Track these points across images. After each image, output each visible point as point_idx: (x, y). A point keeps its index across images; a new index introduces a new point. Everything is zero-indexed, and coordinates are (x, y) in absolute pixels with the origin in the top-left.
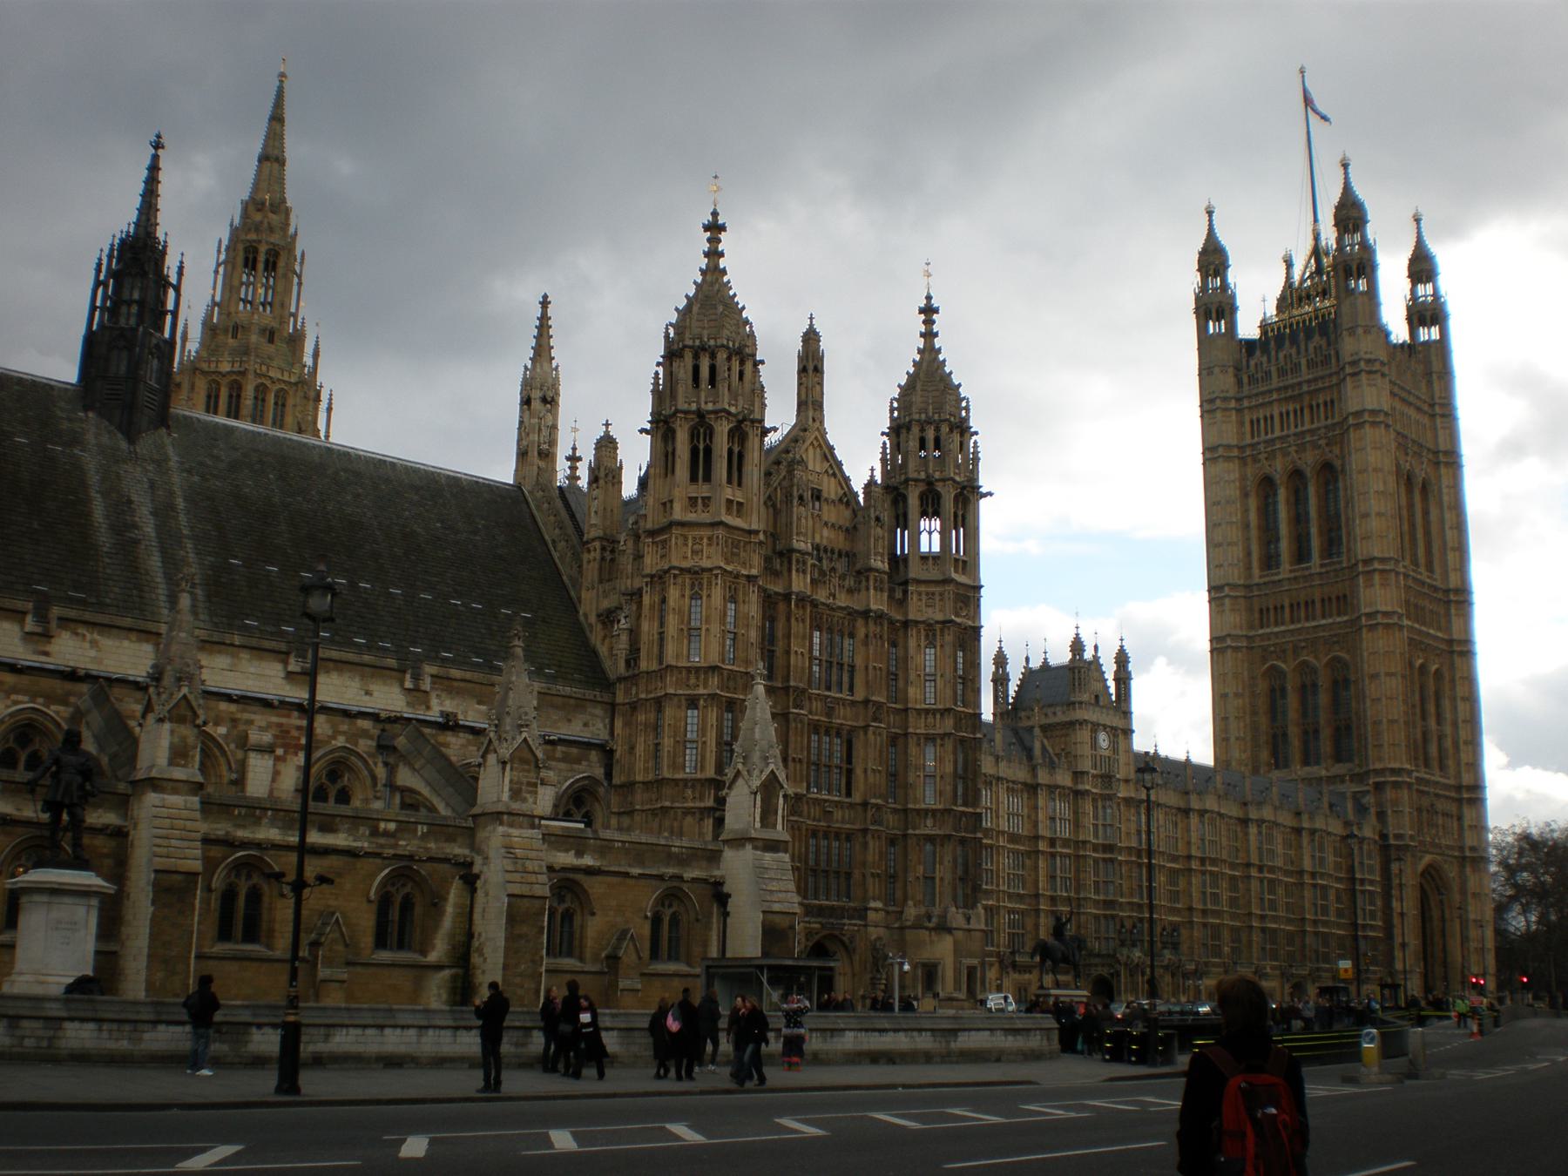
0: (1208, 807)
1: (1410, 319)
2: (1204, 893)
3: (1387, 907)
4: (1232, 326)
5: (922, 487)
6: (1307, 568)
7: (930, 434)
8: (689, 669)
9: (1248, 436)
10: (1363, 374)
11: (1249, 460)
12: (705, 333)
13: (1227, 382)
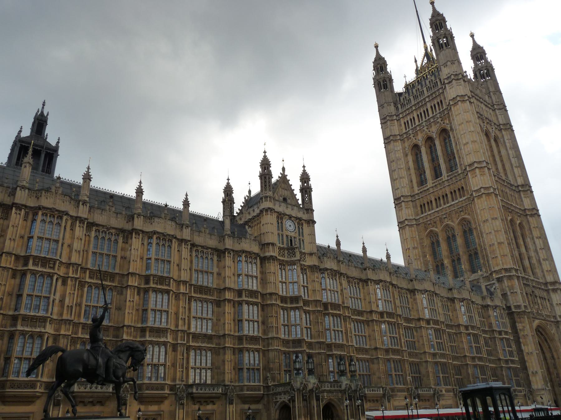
0: (382, 278)
1: (475, 75)
3: (520, 351)
11: (406, 139)
13: (392, 109)
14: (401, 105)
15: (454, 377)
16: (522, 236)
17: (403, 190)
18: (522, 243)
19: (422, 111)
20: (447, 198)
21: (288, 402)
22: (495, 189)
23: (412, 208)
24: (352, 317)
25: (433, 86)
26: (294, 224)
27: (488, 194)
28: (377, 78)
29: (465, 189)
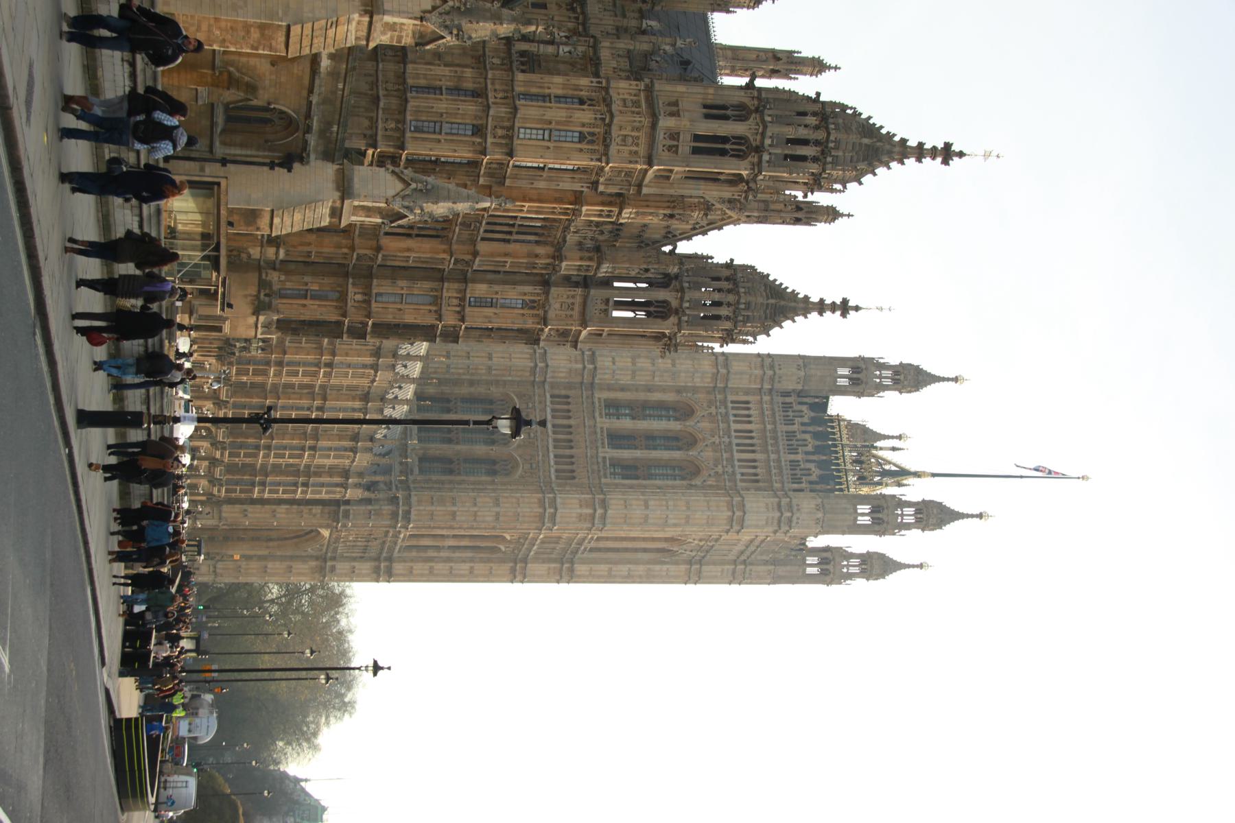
1: (827, 549)
4: (842, 391)
5: (674, 304)
6: (603, 443)
7: (724, 311)
8: (512, 128)
10: (778, 514)
12: (840, 153)
16: (479, 547)
17: (607, 371)
20: (566, 448)
29: (569, 481)
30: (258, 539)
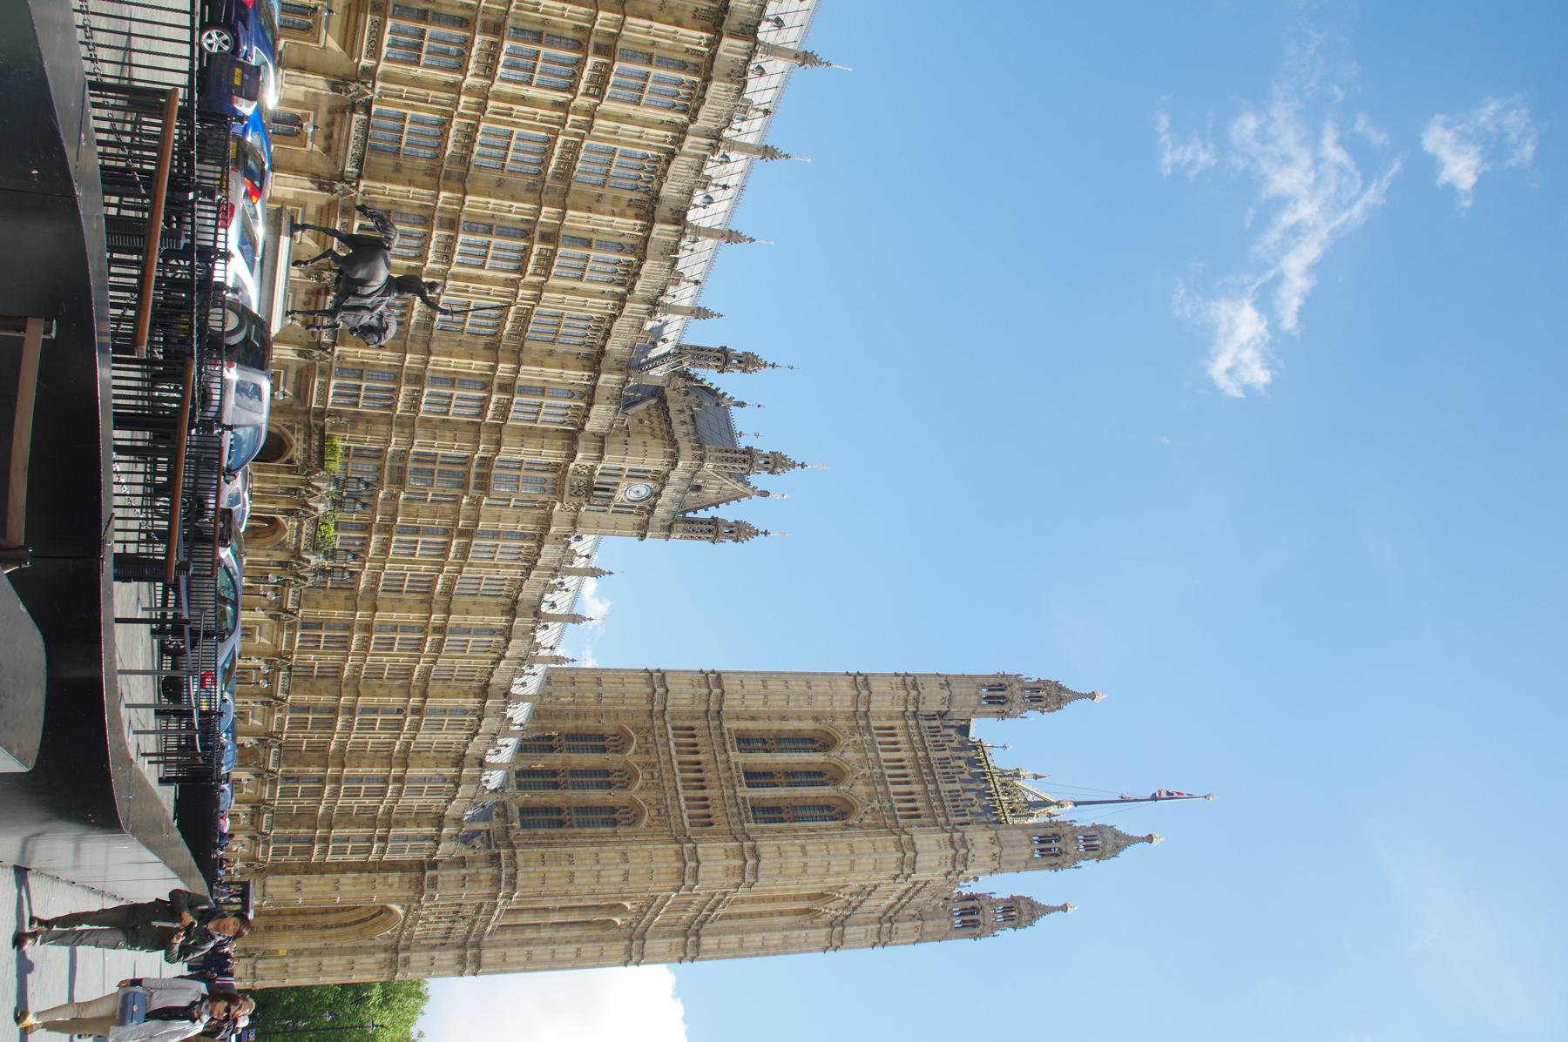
1: (971, 898)
2: (394, 629)
3: (345, 868)
6: (739, 782)
9: (877, 724)
10: (953, 852)
11: (854, 723)
13: (932, 705)
14: (938, 727)
15: (304, 737)
18: (570, 919)
19: (908, 771)
20: (696, 788)
21: (288, 457)
22: (691, 890)
23: (690, 708)
24: (441, 576)
25: (958, 806)
26: (642, 500)
27: (681, 874)
28: (1016, 686)
29: (706, 828)
30: (310, 927)
